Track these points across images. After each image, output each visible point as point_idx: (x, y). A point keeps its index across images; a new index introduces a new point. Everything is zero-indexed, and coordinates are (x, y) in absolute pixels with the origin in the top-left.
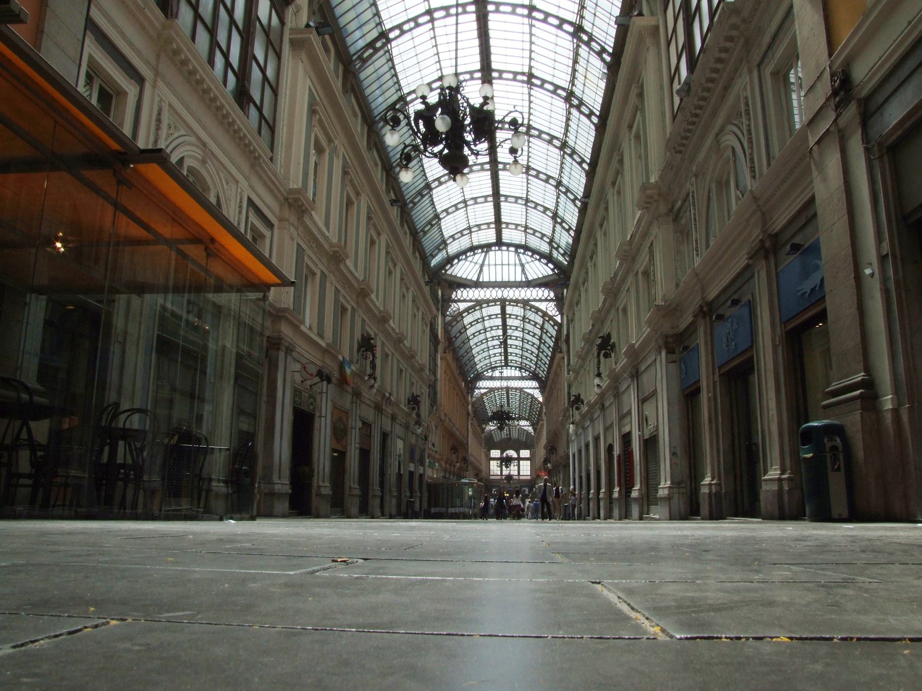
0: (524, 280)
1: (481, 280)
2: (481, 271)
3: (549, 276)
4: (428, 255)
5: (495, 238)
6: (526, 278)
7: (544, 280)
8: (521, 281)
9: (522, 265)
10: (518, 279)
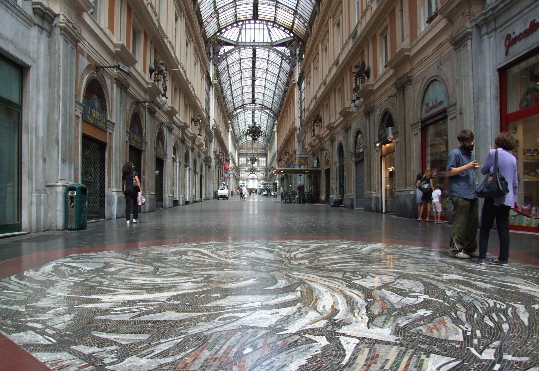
0: (270, 41)
1: (240, 41)
2: (240, 33)
3: (287, 38)
4: (204, 21)
5: (252, 13)
6: (271, 40)
7: (282, 42)
8: (268, 43)
9: (269, 31)
10: (266, 41)
